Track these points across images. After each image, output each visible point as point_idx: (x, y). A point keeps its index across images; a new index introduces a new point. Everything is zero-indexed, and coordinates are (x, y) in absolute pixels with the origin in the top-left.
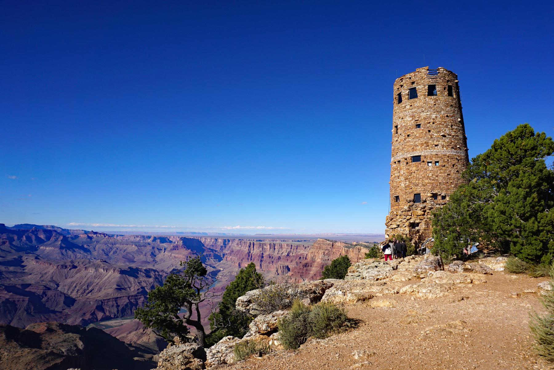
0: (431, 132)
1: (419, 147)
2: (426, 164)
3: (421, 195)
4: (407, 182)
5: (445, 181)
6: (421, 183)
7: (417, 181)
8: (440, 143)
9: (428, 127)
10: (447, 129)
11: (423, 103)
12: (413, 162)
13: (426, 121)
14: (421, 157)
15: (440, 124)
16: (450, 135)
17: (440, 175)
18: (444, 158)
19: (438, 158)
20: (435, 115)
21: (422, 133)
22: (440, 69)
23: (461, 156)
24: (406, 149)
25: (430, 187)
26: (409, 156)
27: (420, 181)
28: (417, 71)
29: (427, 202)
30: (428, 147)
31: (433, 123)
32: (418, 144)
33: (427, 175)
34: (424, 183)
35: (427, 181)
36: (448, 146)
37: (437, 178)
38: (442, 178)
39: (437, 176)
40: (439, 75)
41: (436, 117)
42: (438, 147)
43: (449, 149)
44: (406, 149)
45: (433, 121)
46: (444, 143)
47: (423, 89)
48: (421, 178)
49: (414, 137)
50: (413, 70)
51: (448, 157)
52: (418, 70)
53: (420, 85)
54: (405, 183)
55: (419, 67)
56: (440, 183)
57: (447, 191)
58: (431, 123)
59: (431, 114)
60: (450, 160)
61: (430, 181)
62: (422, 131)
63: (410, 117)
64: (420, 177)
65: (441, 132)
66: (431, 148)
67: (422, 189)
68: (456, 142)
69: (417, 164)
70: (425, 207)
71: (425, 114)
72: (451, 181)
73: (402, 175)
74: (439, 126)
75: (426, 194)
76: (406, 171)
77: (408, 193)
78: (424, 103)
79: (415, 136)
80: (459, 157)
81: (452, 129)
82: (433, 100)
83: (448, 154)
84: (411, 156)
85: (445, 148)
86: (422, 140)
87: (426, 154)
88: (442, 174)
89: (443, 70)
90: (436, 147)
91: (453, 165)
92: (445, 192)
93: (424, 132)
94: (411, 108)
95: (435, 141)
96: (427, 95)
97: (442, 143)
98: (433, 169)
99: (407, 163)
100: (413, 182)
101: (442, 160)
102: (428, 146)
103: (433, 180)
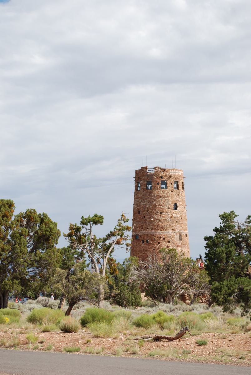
8: (150, 226)
9: (144, 214)
10: (156, 215)
17: (148, 250)
20: (149, 205)
21: (140, 218)
31: (147, 211)
35: (140, 254)
37: (146, 253)
39: (146, 251)
47: (143, 184)
48: (137, 252)
51: (155, 237)
58: (146, 211)
59: (146, 204)
60: (156, 239)
62: (140, 217)
71: (143, 204)
74: (150, 213)
80: (164, 235)
81: (160, 216)
82: (148, 193)
85: (153, 230)
90: (148, 229)
93: (142, 218)
101: (151, 239)
102: (143, 228)
103: (144, 254)
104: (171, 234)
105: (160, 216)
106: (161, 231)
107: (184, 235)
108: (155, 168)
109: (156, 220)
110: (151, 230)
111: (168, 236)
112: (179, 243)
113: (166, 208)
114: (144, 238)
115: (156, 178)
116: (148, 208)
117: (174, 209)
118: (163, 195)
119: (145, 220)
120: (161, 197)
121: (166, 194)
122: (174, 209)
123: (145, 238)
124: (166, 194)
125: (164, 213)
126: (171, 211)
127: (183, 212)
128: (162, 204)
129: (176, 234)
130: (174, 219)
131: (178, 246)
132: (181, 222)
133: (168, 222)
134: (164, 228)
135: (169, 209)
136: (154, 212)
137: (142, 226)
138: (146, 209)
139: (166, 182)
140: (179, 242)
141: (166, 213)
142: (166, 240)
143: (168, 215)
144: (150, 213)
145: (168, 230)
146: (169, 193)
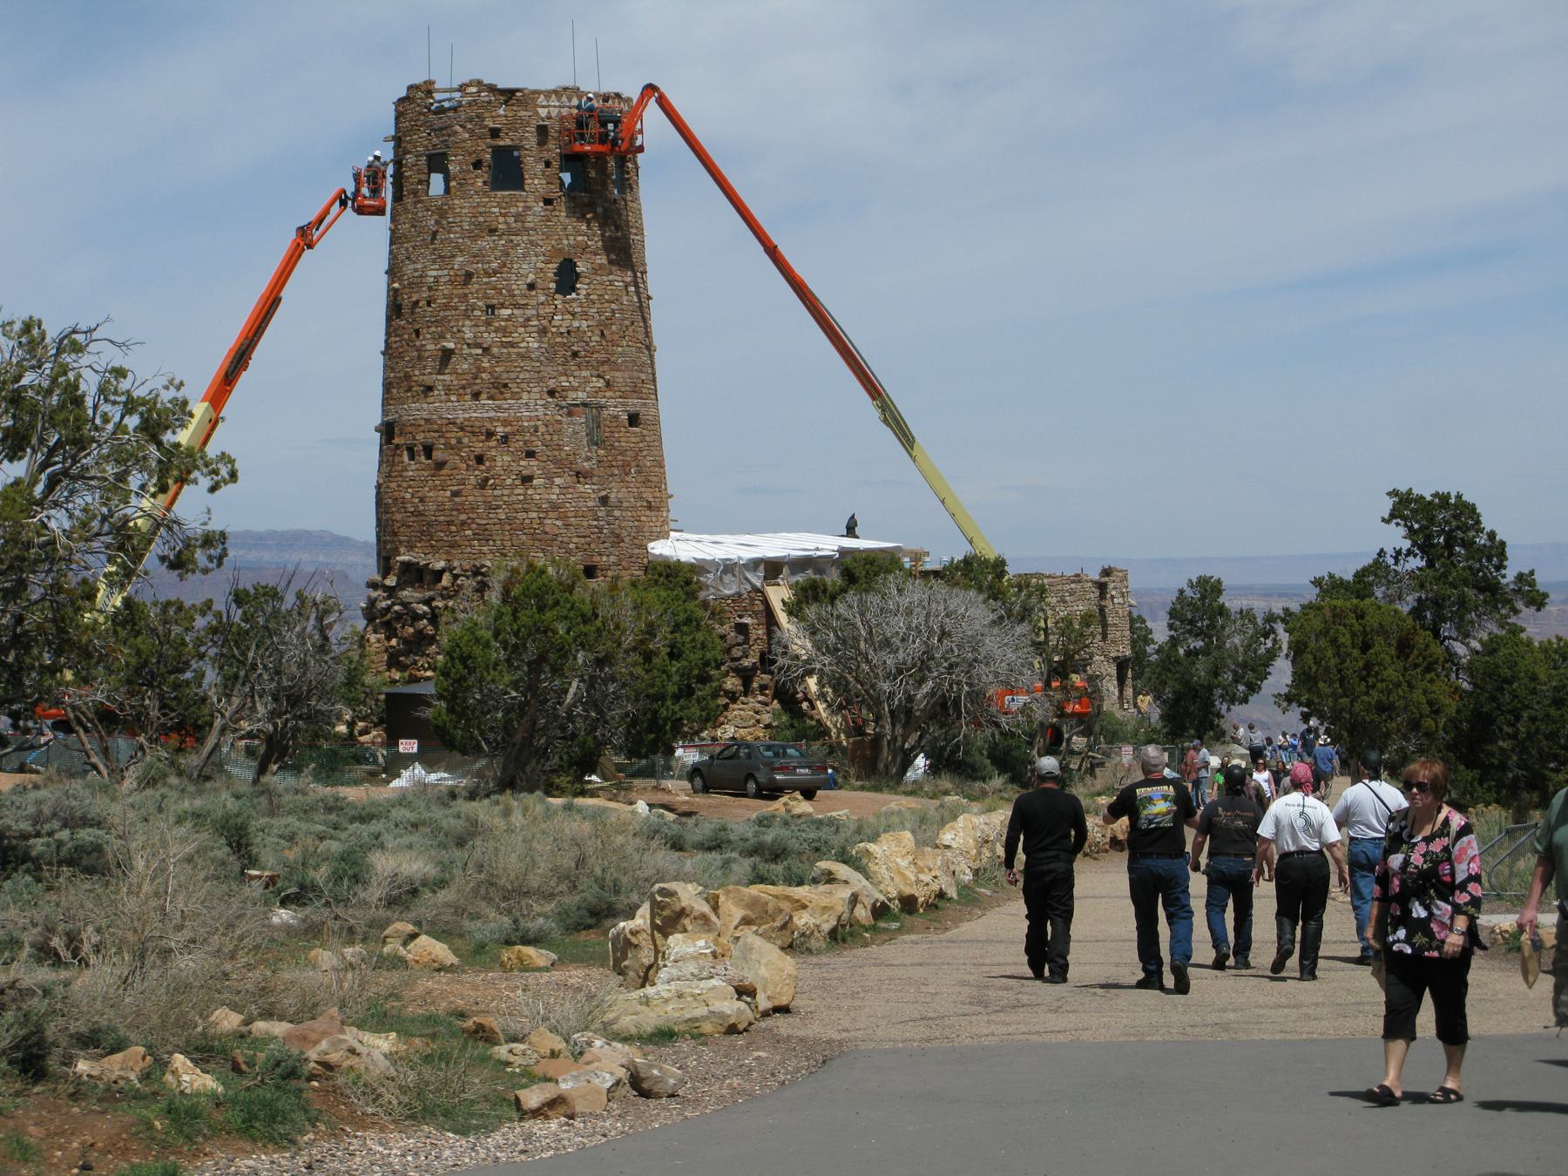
5: (442, 518)
10: (468, 323)
15: (446, 307)
16: (478, 346)
18: (448, 435)
20: (434, 273)
22: (467, 85)
23: (519, 419)
31: (429, 304)
42: (436, 392)
46: (453, 378)
51: (462, 429)
60: (466, 440)
65: (448, 336)
71: (411, 267)
72: (463, 517)
74: (441, 314)
80: (506, 423)
81: (488, 323)
83: (461, 416)
89: (474, 90)
101: (442, 441)
102: (409, 389)
104: (540, 413)
105: (488, 323)
106: (489, 398)
107: (616, 417)
108: (462, 88)
109: (468, 345)
110: (444, 397)
111: (526, 424)
112: (588, 459)
113: (519, 287)
114: (414, 439)
115: (467, 135)
116: (430, 289)
117: (558, 291)
118: (501, 219)
119: (420, 350)
120: (492, 231)
121: (519, 217)
122: (558, 291)
123: (420, 437)
124: (519, 217)
125: (506, 312)
126: (542, 298)
127: (614, 306)
128: (495, 265)
129: (570, 414)
130: (559, 340)
131: (578, 474)
132: (601, 356)
133: (522, 357)
134: (506, 386)
135: (533, 293)
136: (456, 309)
137: (407, 377)
139: (519, 157)
140: (584, 452)
141: (516, 312)
142: (517, 444)
143: (528, 319)
144: (441, 314)
145: (525, 396)
146: (529, 208)
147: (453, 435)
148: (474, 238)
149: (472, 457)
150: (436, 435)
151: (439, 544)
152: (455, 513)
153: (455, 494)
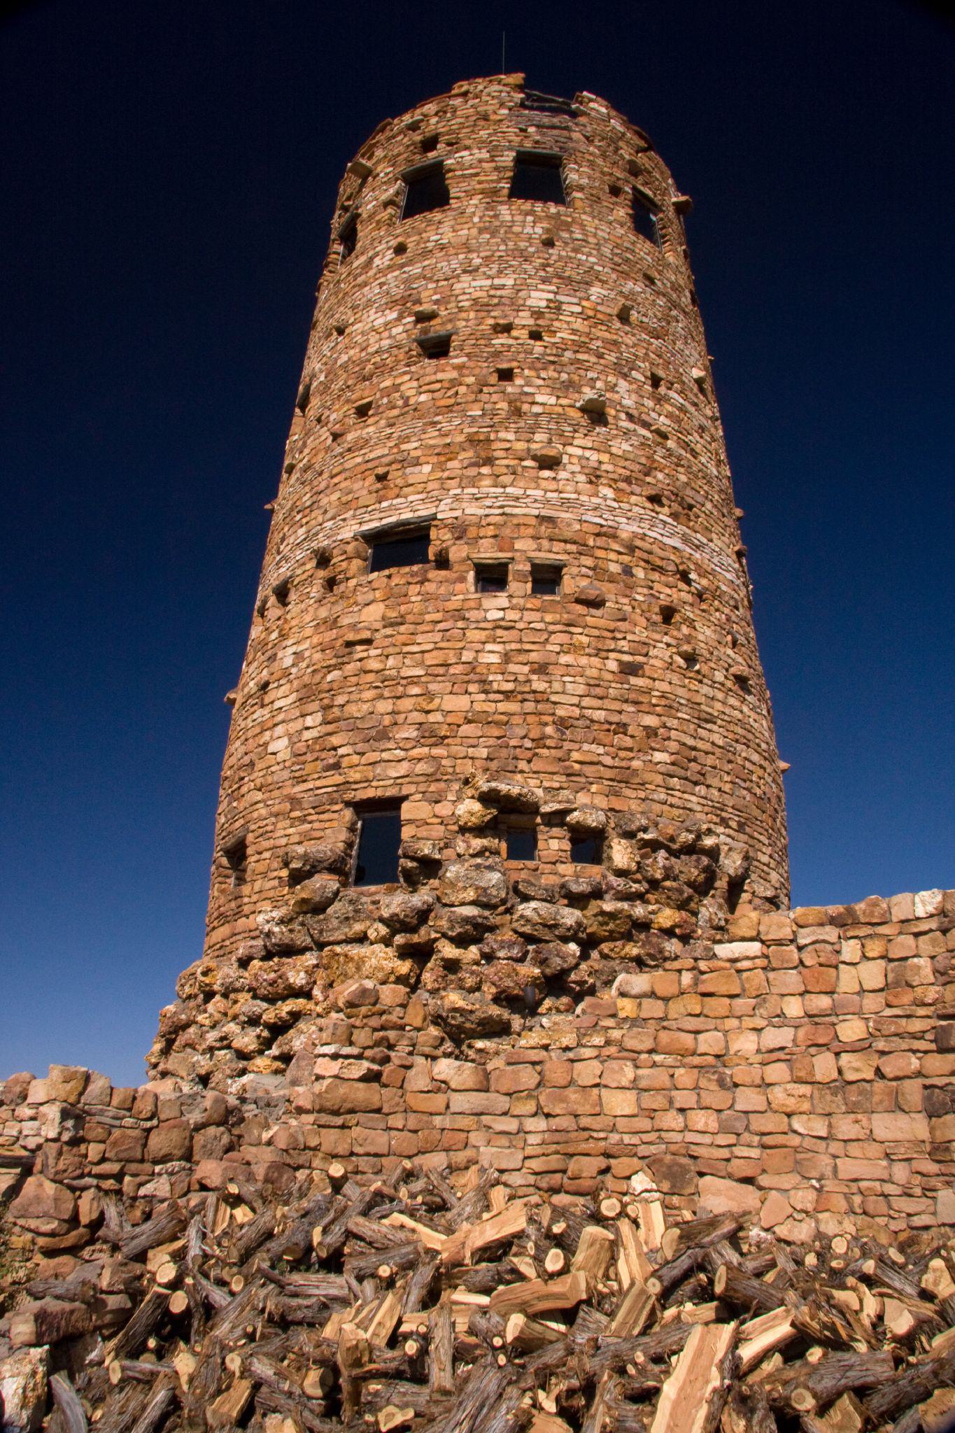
0: (519, 381)
1: (427, 469)
2: (462, 579)
3: (407, 811)
4: (309, 721)
5: (599, 715)
6: (417, 717)
7: (384, 706)
8: (570, 450)
9: (497, 354)
10: (623, 385)
11: (474, 231)
12: (372, 571)
13: (491, 322)
14: (433, 534)
15: (580, 347)
16: (646, 425)
17: (564, 659)
19: (558, 546)
20: (551, 296)
21: (454, 383)
24: (334, 497)
25: (484, 753)
26: (347, 534)
27: (406, 704)
28: (453, 92)
29: (452, 871)
30: (485, 470)
32: (414, 454)
33: (467, 656)
34: (432, 718)
36: (628, 480)
37: (539, 684)
38: (581, 689)
39: (541, 669)
40: (582, 120)
41: (556, 307)
42: (563, 475)
43: (634, 499)
44: (334, 497)
45: (531, 322)
46: (605, 457)
47: (485, 165)
48: (413, 681)
49: (396, 412)
50: (439, 86)
51: (631, 549)
52: (464, 89)
53: (467, 148)
54: (295, 726)
55: (469, 75)
56: (563, 724)
57: (617, 794)
58: (523, 334)
60: (640, 573)
61: (481, 703)
62: (454, 374)
63: (392, 304)
64: (407, 672)
66: (507, 479)
67: (421, 768)
68: (683, 478)
69: (395, 581)
70: (423, 915)
71: (489, 282)
72: (650, 721)
73: (286, 673)
74: (568, 354)
75: (444, 809)
76: (315, 640)
77: (308, 800)
78: (481, 231)
79: (406, 404)
83: (627, 529)
84: (365, 527)
86: (446, 427)
87: (472, 509)
88: (584, 661)
90: (546, 473)
91: (668, 614)
92: (601, 802)
93: (471, 380)
94: (401, 260)
95: (537, 437)
96: (506, 192)
97: (588, 454)
98: (512, 615)
99: (331, 584)
100: (352, 709)
101: (589, 562)
102: (489, 461)
103: (508, 695)
111: (724, 588)
138: (524, 319)
147: (613, 556)
148: (625, 275)
149: (657, 610)
150: (569, 547)
151: (589, 770)
152: (632, 709)
153: (630, 670)
